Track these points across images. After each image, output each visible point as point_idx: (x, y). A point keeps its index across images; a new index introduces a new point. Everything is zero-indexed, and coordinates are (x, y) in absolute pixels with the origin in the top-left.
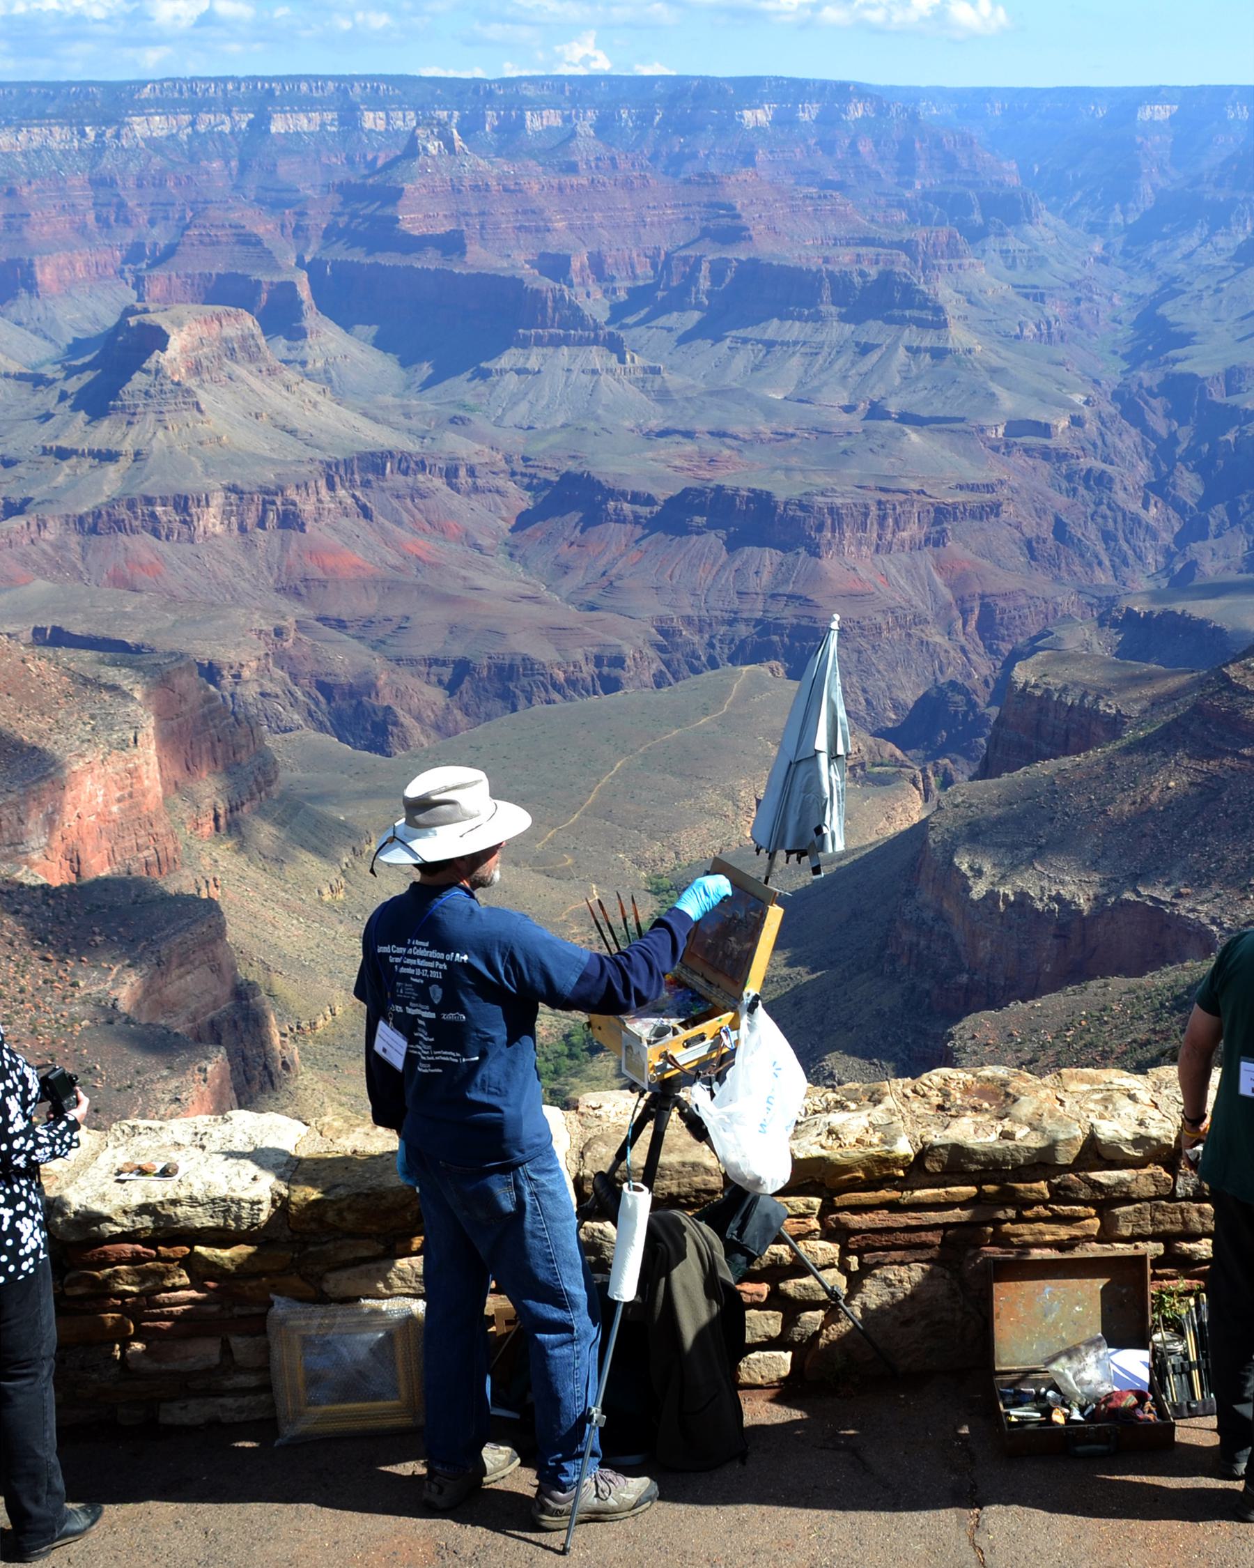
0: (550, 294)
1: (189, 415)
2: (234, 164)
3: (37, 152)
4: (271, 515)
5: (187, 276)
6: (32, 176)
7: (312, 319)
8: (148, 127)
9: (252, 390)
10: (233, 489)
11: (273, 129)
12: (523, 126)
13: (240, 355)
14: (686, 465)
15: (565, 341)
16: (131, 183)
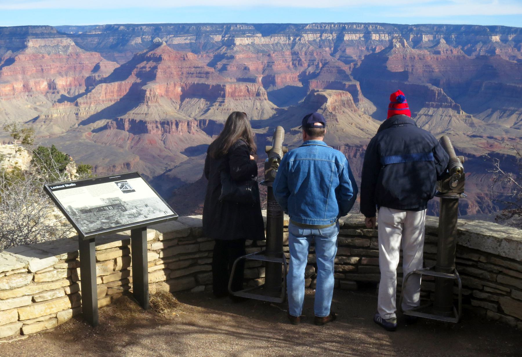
0: (437, 92)
1: (334, 123)
2: (332, 49)
3: (276, 44)
4: (358, 154)
5: (323, 82)
6: (275, 51)
7: (361, 96)
8: (309, 37)
9: (350, 116)
10: (347, 145)
11: (345, 39)
12: (422, 39)
13: (346, 105)
14: (483, 146)
15: (441, 106)
16: (303, 54)
